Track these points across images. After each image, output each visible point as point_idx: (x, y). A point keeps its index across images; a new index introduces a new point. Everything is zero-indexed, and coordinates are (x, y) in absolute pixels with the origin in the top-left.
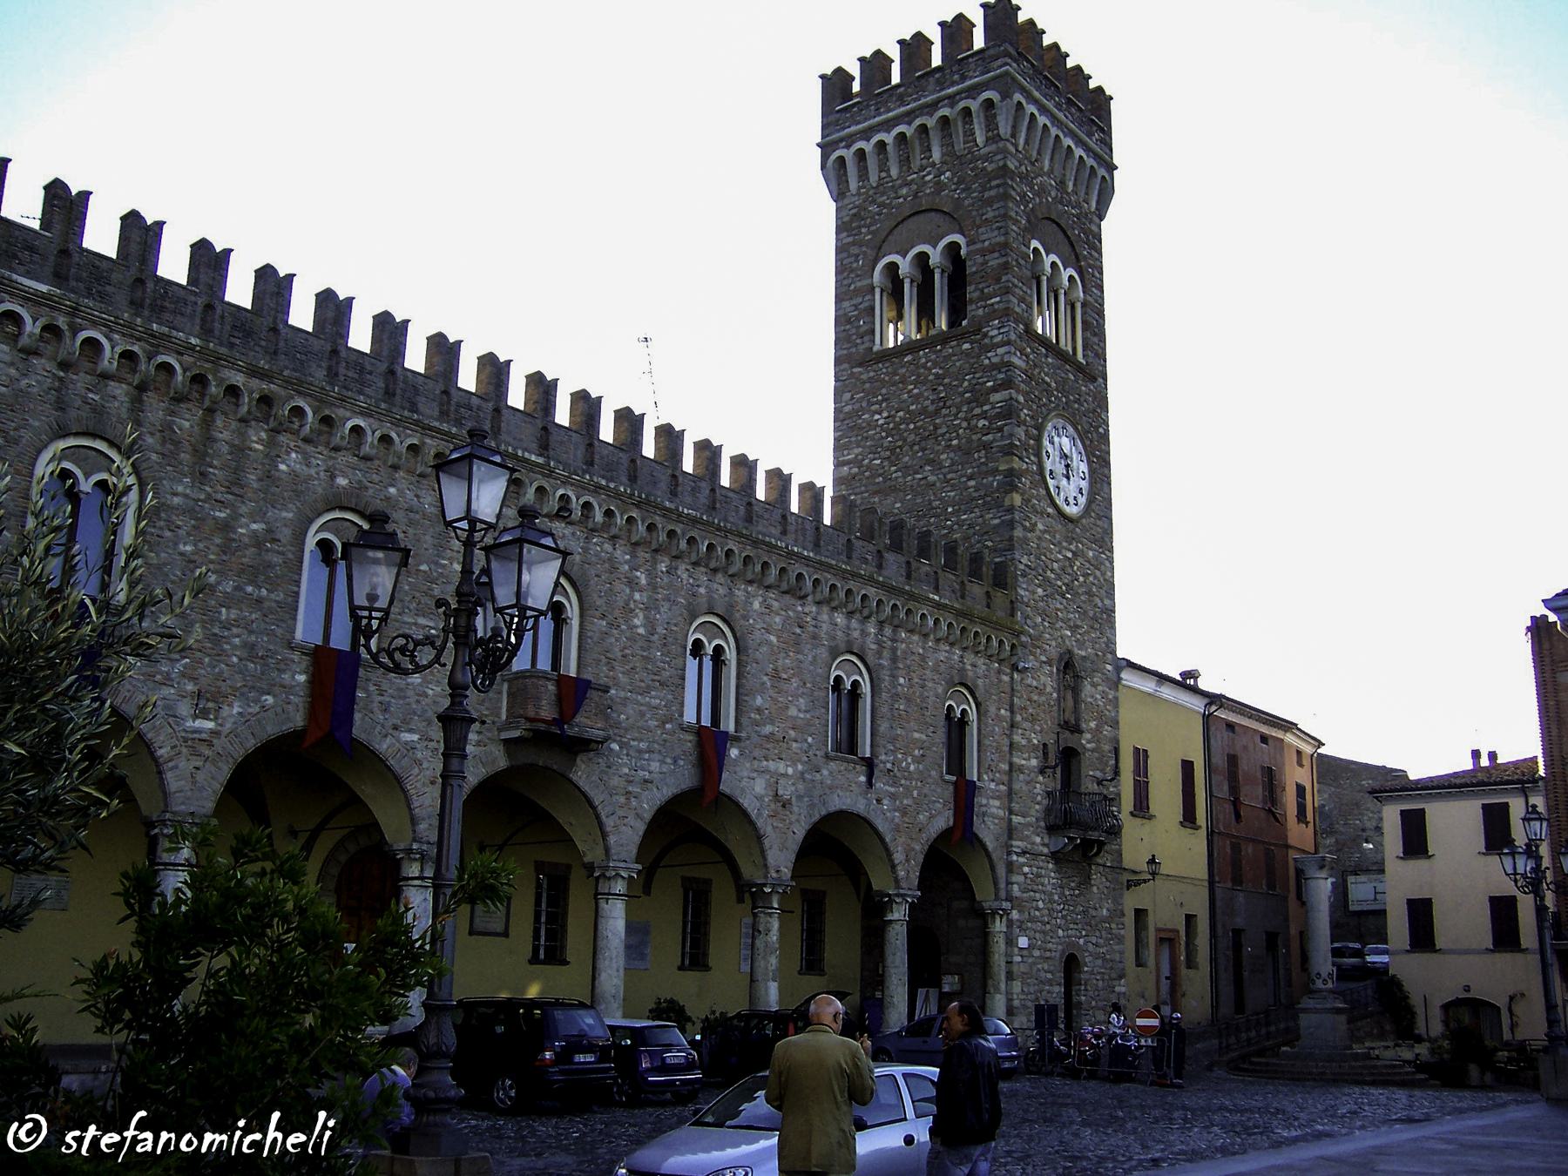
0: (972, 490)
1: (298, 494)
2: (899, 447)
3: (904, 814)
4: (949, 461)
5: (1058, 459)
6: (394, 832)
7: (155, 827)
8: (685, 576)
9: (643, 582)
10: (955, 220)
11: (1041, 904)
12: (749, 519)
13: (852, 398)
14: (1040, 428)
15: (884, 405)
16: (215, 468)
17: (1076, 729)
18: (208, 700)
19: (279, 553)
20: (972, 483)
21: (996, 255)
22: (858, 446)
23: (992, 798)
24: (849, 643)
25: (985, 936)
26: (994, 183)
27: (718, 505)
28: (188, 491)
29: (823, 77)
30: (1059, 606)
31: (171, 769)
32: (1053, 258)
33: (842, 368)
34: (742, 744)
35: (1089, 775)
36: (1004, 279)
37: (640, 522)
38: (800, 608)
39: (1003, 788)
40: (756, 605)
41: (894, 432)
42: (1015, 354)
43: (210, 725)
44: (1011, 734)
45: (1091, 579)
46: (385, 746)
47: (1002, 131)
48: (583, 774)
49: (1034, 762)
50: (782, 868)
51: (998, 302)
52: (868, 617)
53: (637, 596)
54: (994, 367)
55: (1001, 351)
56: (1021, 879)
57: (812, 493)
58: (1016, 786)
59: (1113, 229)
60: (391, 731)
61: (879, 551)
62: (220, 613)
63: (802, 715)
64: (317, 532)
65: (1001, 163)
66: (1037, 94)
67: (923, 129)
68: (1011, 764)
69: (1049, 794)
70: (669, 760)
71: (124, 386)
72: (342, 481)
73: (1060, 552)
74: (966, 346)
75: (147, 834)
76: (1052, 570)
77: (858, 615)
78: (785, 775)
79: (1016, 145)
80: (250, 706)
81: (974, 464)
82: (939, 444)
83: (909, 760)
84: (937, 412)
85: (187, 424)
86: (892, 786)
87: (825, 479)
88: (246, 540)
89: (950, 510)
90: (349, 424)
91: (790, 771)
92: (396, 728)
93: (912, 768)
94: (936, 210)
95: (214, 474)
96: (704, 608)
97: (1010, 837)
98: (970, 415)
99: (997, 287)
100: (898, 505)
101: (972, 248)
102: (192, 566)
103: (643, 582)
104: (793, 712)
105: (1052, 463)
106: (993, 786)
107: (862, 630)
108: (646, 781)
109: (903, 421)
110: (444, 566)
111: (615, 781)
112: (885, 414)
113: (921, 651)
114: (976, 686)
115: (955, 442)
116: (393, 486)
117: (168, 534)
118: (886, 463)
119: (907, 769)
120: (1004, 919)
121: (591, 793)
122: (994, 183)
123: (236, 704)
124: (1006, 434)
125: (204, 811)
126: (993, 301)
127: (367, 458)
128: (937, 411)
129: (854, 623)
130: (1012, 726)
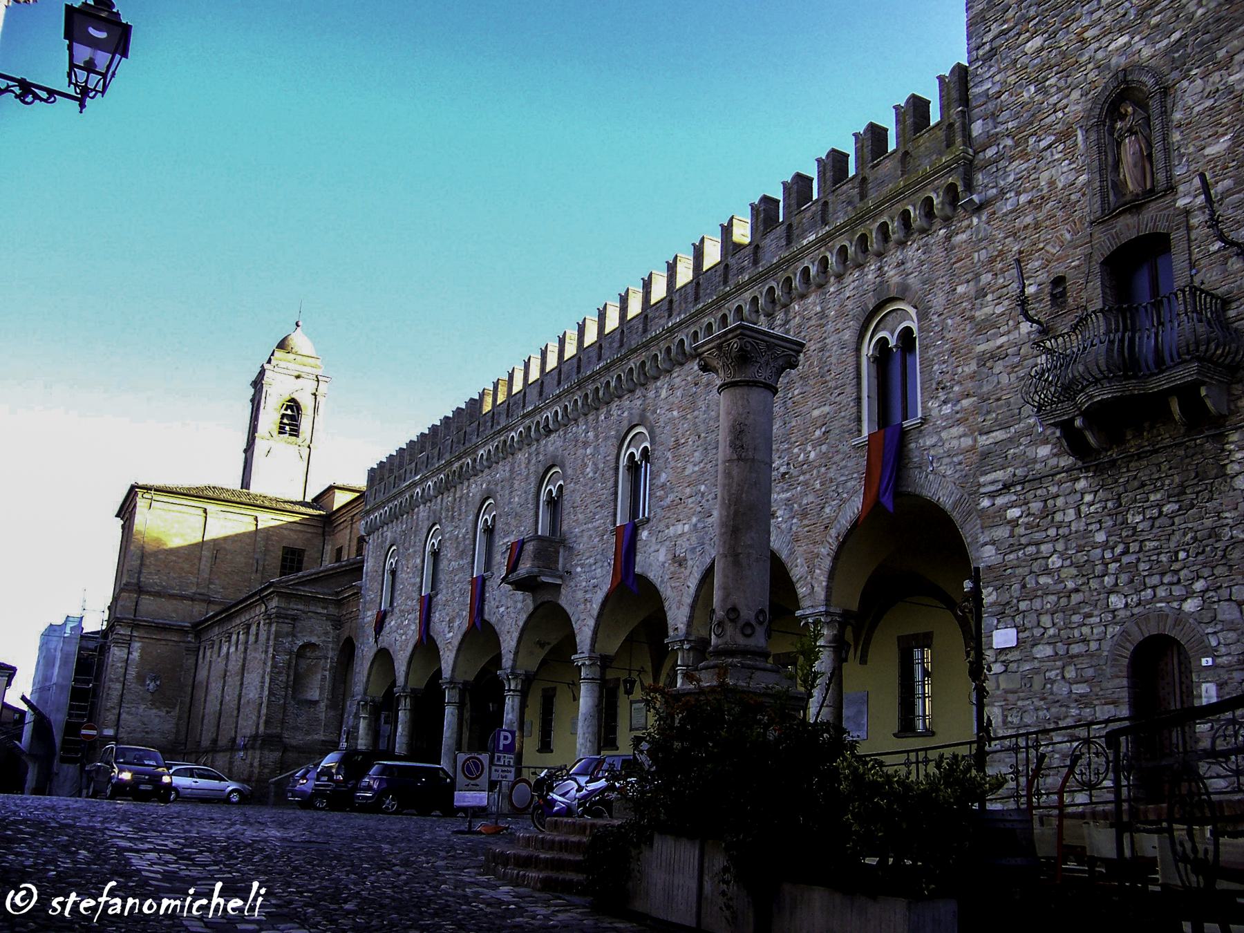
11: (1055, 562)
23: (945, 428)
39: (965, 403)
50: (678, 625)
86: (787, 491)
106: (947, 409)
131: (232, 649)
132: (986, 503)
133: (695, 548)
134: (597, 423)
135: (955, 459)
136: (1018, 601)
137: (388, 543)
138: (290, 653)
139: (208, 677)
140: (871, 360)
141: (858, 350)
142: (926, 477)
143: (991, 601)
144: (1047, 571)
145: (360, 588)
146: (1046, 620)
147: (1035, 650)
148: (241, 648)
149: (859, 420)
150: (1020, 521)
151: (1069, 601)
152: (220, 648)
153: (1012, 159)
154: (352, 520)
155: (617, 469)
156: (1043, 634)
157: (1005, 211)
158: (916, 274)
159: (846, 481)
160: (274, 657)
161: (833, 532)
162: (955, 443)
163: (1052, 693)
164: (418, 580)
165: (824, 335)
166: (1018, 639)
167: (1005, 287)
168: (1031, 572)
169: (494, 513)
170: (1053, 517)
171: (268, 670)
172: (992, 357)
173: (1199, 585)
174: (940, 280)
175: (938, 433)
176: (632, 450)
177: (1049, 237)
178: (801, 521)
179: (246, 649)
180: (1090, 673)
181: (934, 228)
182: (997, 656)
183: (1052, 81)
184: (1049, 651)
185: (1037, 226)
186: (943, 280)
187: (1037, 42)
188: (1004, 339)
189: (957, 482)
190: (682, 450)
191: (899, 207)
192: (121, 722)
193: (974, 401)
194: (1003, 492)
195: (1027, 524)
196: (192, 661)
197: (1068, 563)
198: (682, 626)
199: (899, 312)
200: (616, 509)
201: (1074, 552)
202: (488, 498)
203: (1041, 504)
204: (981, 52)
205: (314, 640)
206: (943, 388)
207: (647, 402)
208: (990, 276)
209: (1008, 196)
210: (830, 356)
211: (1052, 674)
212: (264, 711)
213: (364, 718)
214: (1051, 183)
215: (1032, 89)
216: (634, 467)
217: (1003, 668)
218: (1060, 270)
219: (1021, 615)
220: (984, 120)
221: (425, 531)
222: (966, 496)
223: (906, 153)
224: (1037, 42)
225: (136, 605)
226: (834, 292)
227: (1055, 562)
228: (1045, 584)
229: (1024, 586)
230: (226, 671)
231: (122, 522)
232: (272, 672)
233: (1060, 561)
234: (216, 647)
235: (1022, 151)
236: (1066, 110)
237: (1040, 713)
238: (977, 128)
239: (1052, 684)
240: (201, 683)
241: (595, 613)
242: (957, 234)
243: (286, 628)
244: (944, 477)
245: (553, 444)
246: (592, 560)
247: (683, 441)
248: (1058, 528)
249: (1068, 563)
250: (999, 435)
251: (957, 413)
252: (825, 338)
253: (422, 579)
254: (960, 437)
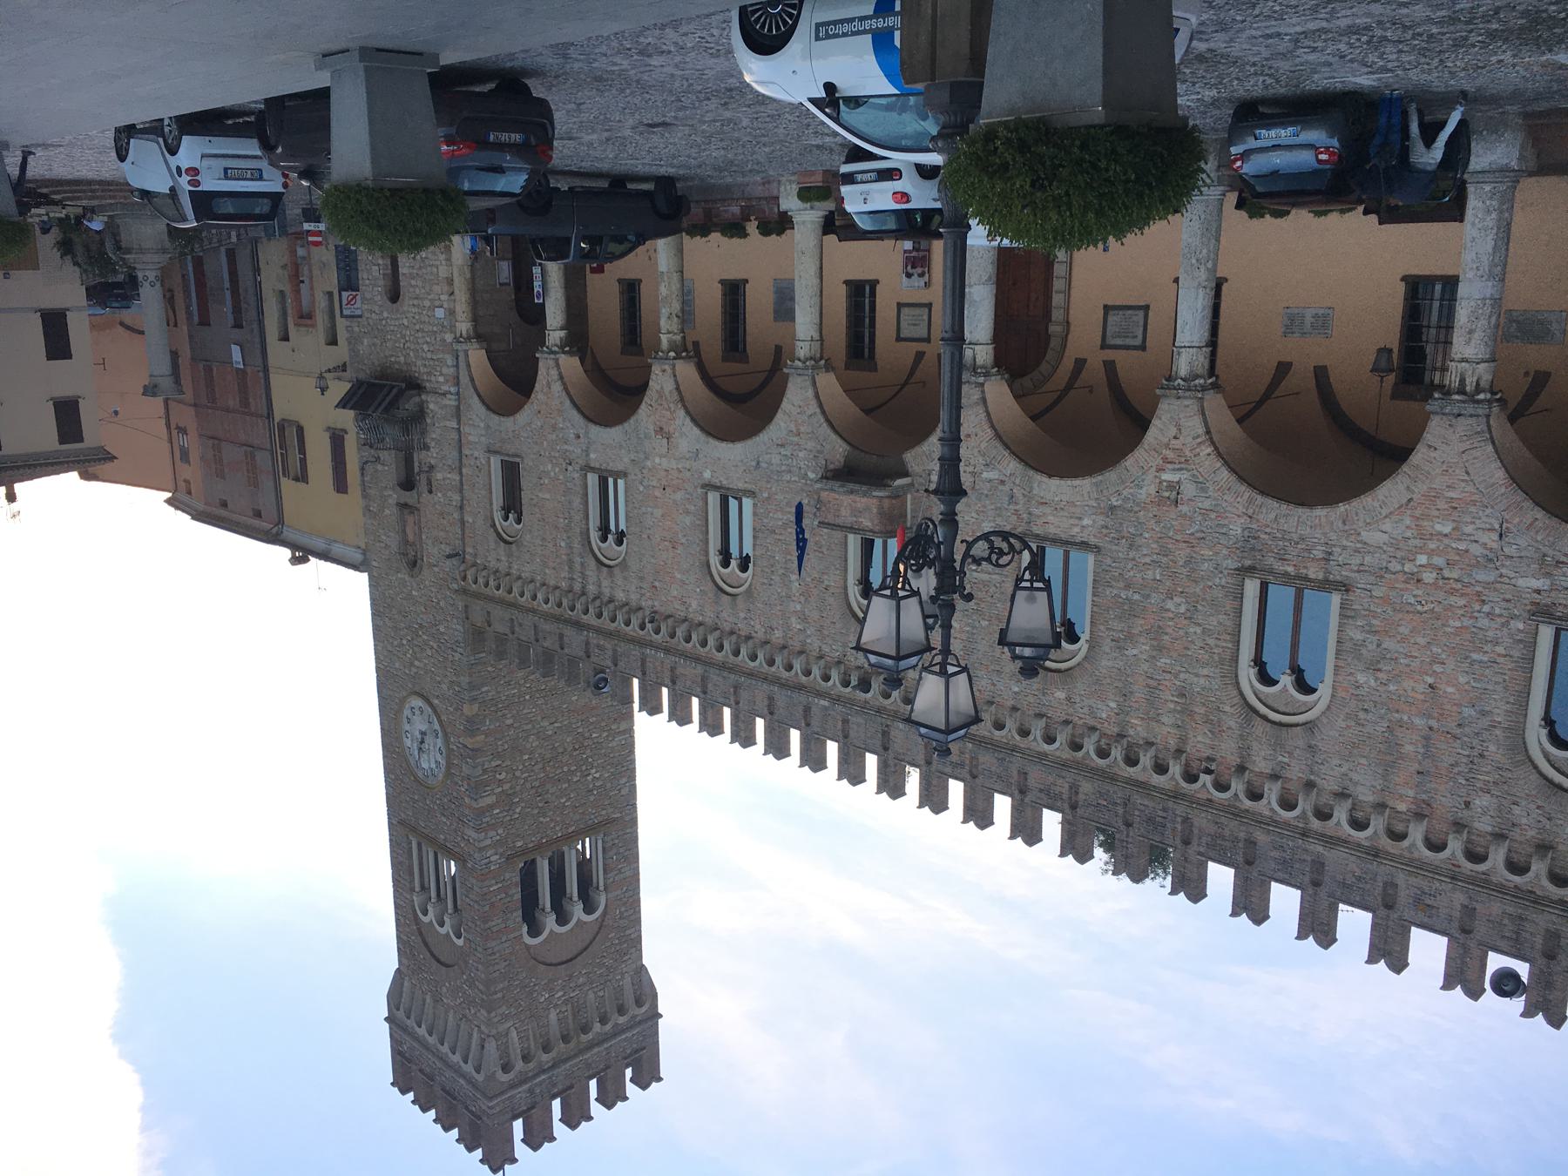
0: (509, 716)
1: (1097, 682)
2: (576, 750)
3: (554, 427)
4: (531, 740)
5: (431, 748)
6: (998, 391)
7: (1211, 384)
8: (758, 627)
9: (793, 620)
10: (534, 957)
11: (425, 347)
12: (704, 679)
13: (620, 790)
14: (448, 774)
15: (591, 786)
16: (1172, 701)
17: (404, 506)
18: (1169, 498)
19: (1114, 630)
20: (509, 722)
21: (495, 929)
22: (613, 747)
24: (611, 575)
25: (475, 319)
26: (499, 995)
27: (732, 690)
28: (1196, 679)
29: (660, 1079)
30: (425, 617)
31: (1198, 436)
32: (442, 931)
33: (630, 817)
34: (701, 482)
35: (388, 466)
36: (487, 908)
37: (799, 671)
38: (656, 604)
40: (694, 604)
41: (582, 763)
42: (475, 840)
43: (1165, 476)
44: (462, 500)
45: (396, 643)
46: (1011, 465)
47: (494, 1043)
48: (837, 450)
49: (439, 476)
51: (491, 886)
52: (595, 599)
53: (798, 607)
54: (493, 827)
55: (488, 842)
56: (445, 370)
57: (653, 708)
58: (455, 454)
59: (390, 962)
60: (1007, 479)
61: (589, 657)
62: (1161, 575)
63: (649, 509)
64: (1080, 649)
65: (493, 1014)
66: (462, 1081)
67: (565, 1039)
68: (461, 474)
69: (426, 447)
70: (763, 465)
71: (1257, 770)
72: (1061, 695)
73: (426, 664)
74: (519, 844)
75: (1217, 377)
76: (432, 648)
77: (605, 599)
78: (661, 456)
79: (480, 1031)
80: (1130, 494)
81: (508, 738)
82: (540, 754)
83: (552, 474)
84: (542, 785)
85: (1199, 738)
86: (566, 450)
87: (641, 719)
88: (1142, 640)
89: (527, 697)
90: (1057, 744)
91: (657, 460)
92: (1002, 482)
93: (550, 467)
94: (550, 965)
95: (1173, 695)
96: (740, 600)
97: (458, 408)
98: (514, 782)
99: (494, 899)
100: (575, 698)
101: (517, 934)
102: (1188, 615)
103: (793, 620)
104: (658, 512)
105: (435, 744)
106: (476, 454)
107: (600, 586)
108: (782, 446)
109: (573, 773)
110: (968, 625)
111: (810, 445)
112: (590, 778)
113: (547, 571)
114: (496, 542)
115: (526, 757)
116: (1016, 693)
117: (1211, 642)
118: (587, 735)
120: (458, 335)
121: (829, 431)
122: (499, 995)
123: (1144, 496)
124: (480, 768)
125: (1168, 402)
126: (495, 887)
127: (1040, 716)
128: (542, 785)
129: (607, 591)
130: (461, 508)
144: (427, 343)
173: (384, 322)
180: (411, 290)
227: (425, 347)
250: (448, 423)
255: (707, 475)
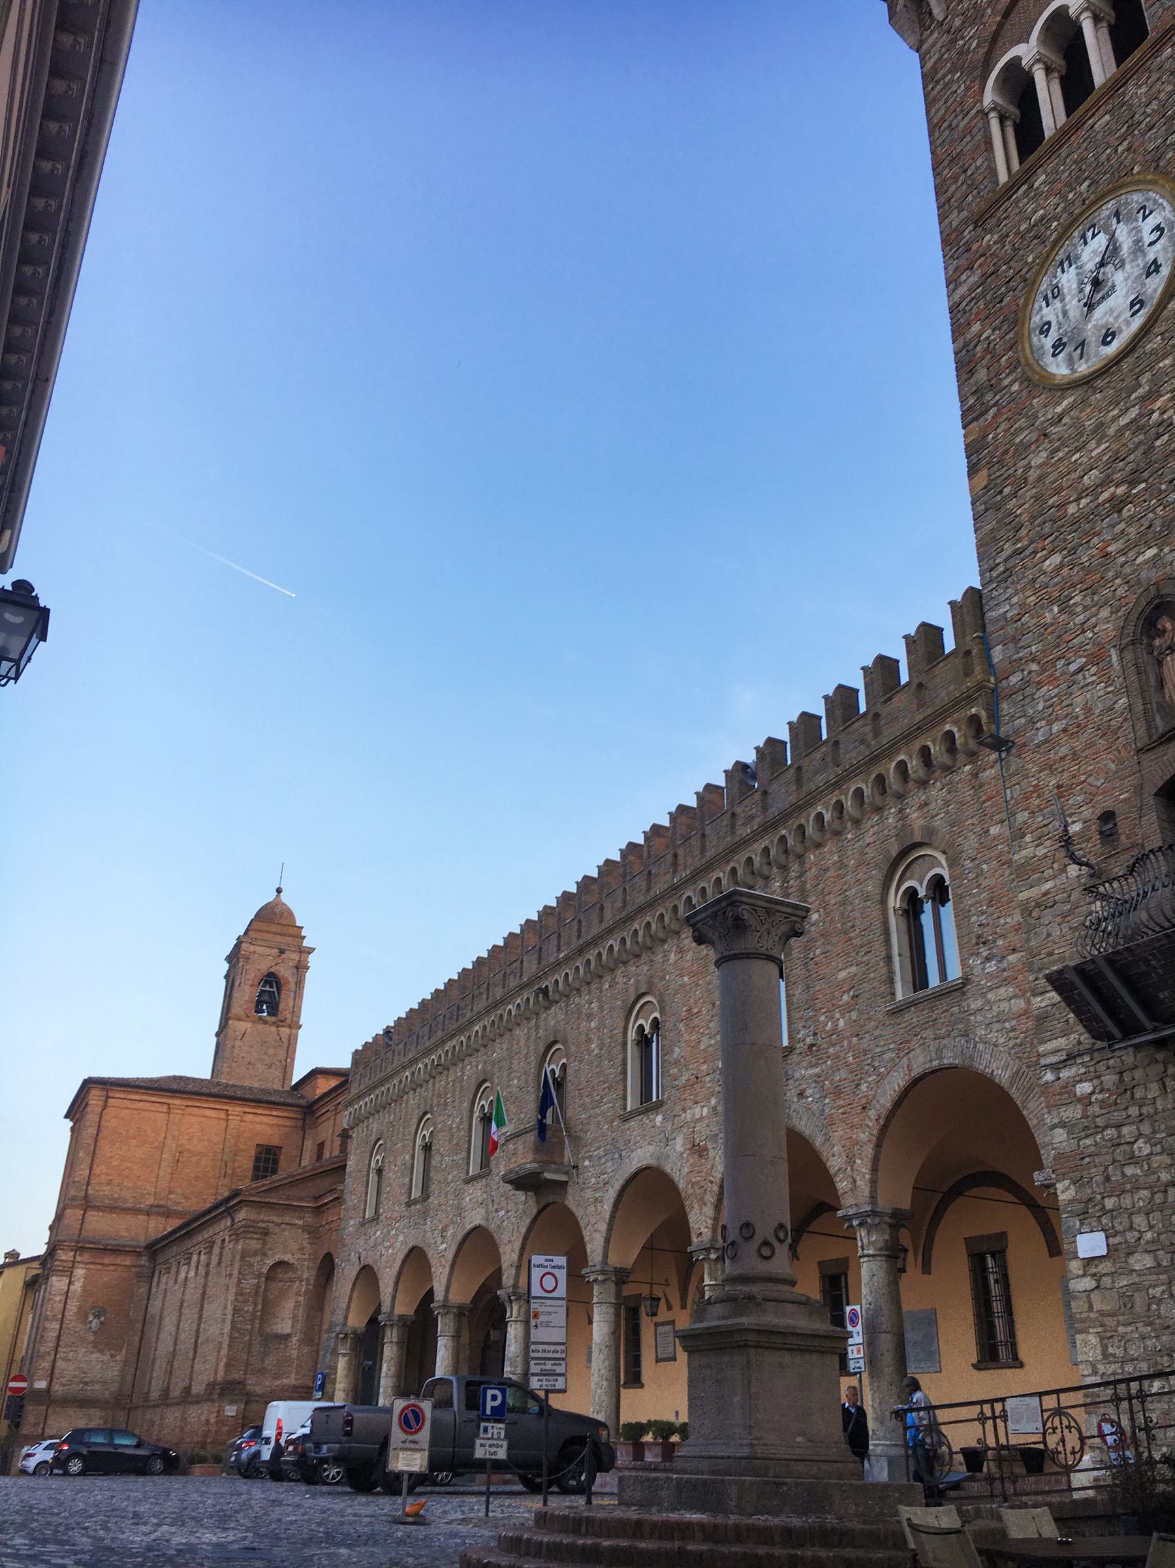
11: (1142, 1148)
23: (991, 989)
39: (1012, 958)
86: (816, 1065)
106: (991, 967)
119: (835, 1031)
131: (192, 1273)
132: (1049, 1076)
133: (717, 1135)
134: (601, 992)
135: (1007, 1025)
136: (1103, 1198)
137: (373, 1138)
138: (259, 1276)
139: (162, 1309)
140: (900, 912)
141: (884, 901)
142: (975, 1047)
143: (1070, 1197)
144: (1133, 1160)
145: (342, 1191)
146: (1140, 1221)
147: (1131, 1260)
148: (202, 1270)
149: (891, 981)
150: (1093, 1098)
151: (1166, 1197)
152: (177, 1272)
153: (1040, 685)
154: (336, 1109)
155: (625, 1044)
156: (1139, 1239)
157: (1036, 742)
158: (943, 815)
159: (883, 1053)
160: (239, 1282)
161: (872, 1114)
162: (1004, 1006)
163: (1159, 1317)
164: (407, 1180)
165: (845, 887)
166: (1108, 1245)
167: (1045, 826)
168: (1114, 1161)
169: (491, 1098)
170: (1133, 1093)
171: (231, 1297)
172: (1038, 905)
174: (970, 821)
175: (984, 995)
176: (641, 1021)
177: (1091, 767)
178: (834, 1100)
179: (207, 1274)
181: (958, 764)
182: (1084, 1267)
183: (1078, 599)
184: (1148, 1261)
185: (1075, 755)
186: (974, 821)
187: (1056, 559)
188: (1049, 885)
189: (1013, 1052)
190: (696, 1021)
191: (917, 745)
192: (56, 1372)
193: (1023, 957)
194: (1069, 1063)
195: (1103, 1101)
196: (143, 1290)
197: (1158, 1148)
198: (706, 1230)
199: (927, 858)
200: (625, 1090)
201: (1164, 1135)
202: (484, 1081)
203: (1115, 1077)
204: (994, 574)
205: (287, 1257)
206: (984, 943)
207: (655, 967)
208: (1026, 813)
209: (1038, 725)
210: (853, 910)
211: (1157, 1292)
212: (224, 1352)
213: (343, 1355)
214: (1088, 710)
215: (1056, 609)
216: (644, 1042)
217: (1094, 1284)
218: (1108, 805)
219: (1109, 1214)
220: (1004, 645)
221: (415, 1121)
222: (1024, 1067)
223: (921, 685)
224: (1056, 559)
225: (82, 1224)
226: (852, 839)
227: (1142, 1148)
228: (1133, 1175)
229: (1107, 1179)
230: (182, 1301)
231: (71, 1124)
232: (236, 1300)
233: (1148, 1146)
234: (174, 1270)
235: (1050, 676)
236: (1096, 630)
237: (1149, 1343)
238: (997, 654)
239: (1158, 1305)
240: (153, 1317)
241: (607, 1216)
242: (985, 769)
243: (255, 1245)
244: (996, 1046)
245: (554, 1017)
246: (601, 1152)
247: (696, 1010)
248: (1140, 1106)
249: (1158, 1148)
251: (1004, 970)
252: (846, 891)
253: (411, 1180)
254: (1011, 999)
255: (659, 1119)
